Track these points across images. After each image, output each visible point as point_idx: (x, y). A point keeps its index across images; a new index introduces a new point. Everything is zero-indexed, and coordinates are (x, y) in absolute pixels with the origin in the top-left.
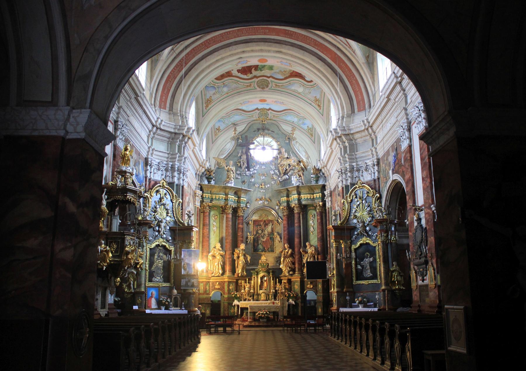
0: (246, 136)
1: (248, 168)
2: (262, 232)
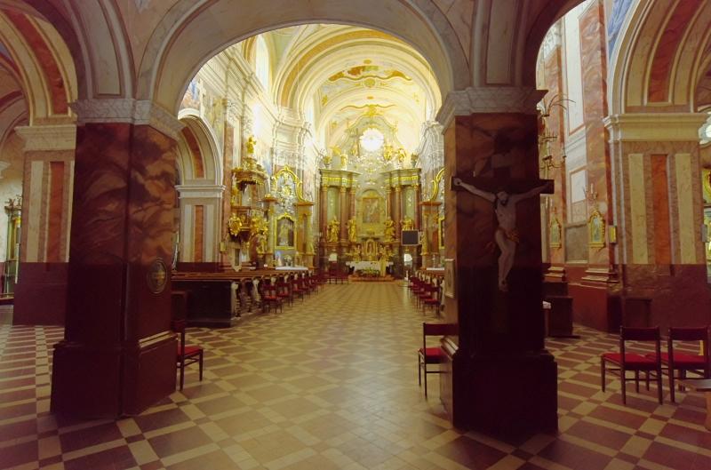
0: (357, 130)
1: (359, 155)
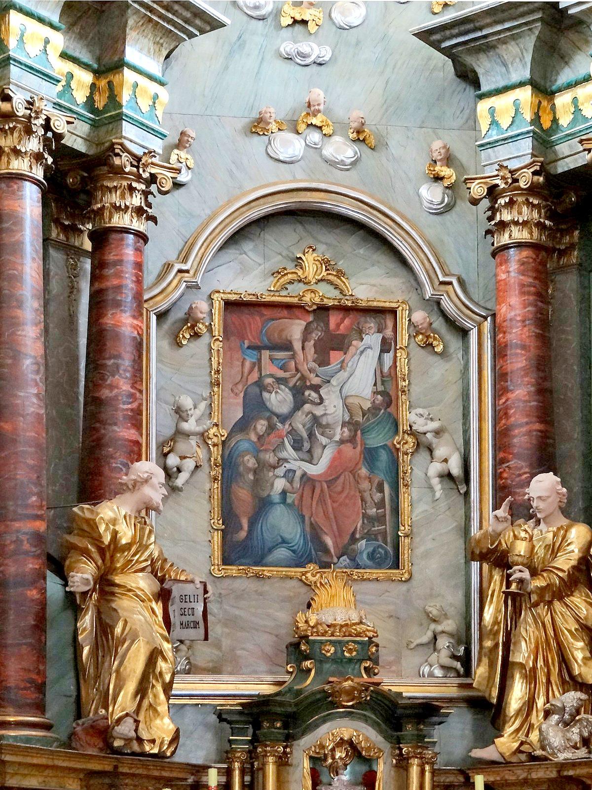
2: (299, 404)
